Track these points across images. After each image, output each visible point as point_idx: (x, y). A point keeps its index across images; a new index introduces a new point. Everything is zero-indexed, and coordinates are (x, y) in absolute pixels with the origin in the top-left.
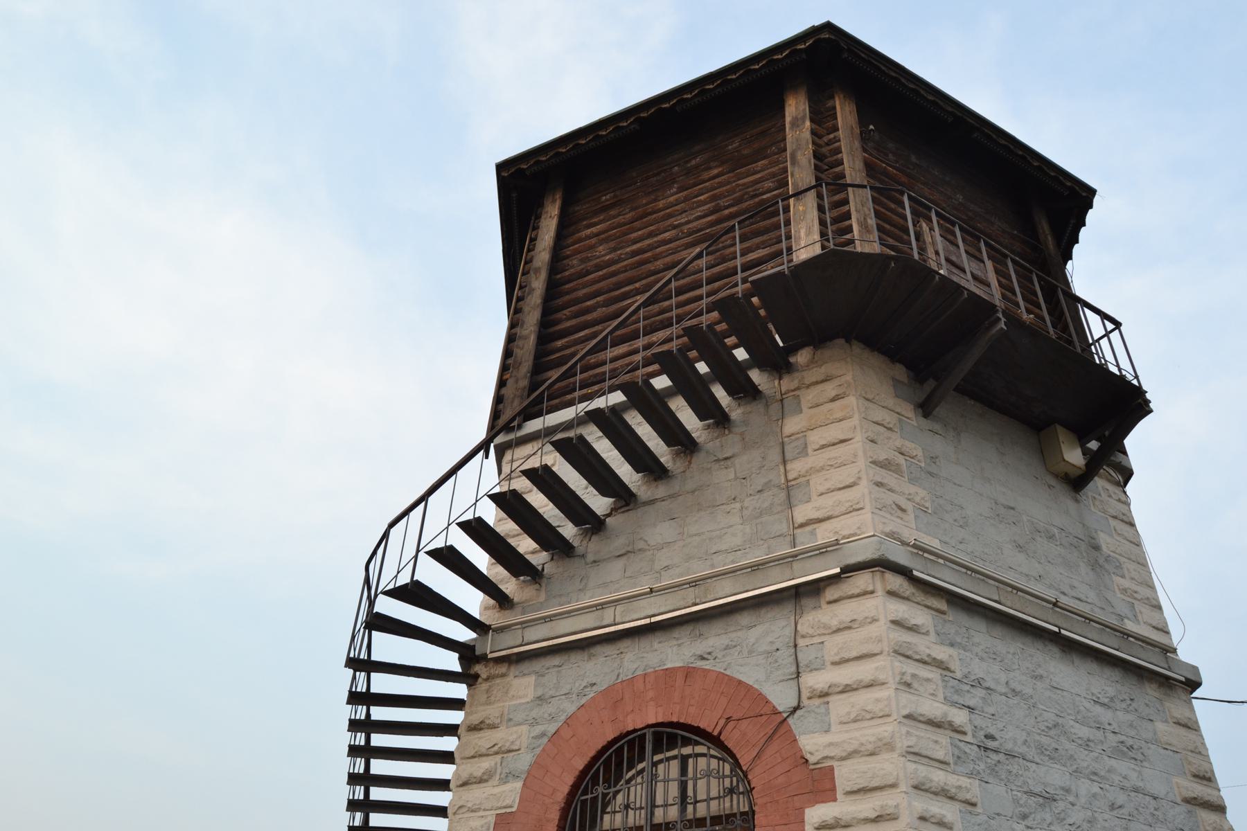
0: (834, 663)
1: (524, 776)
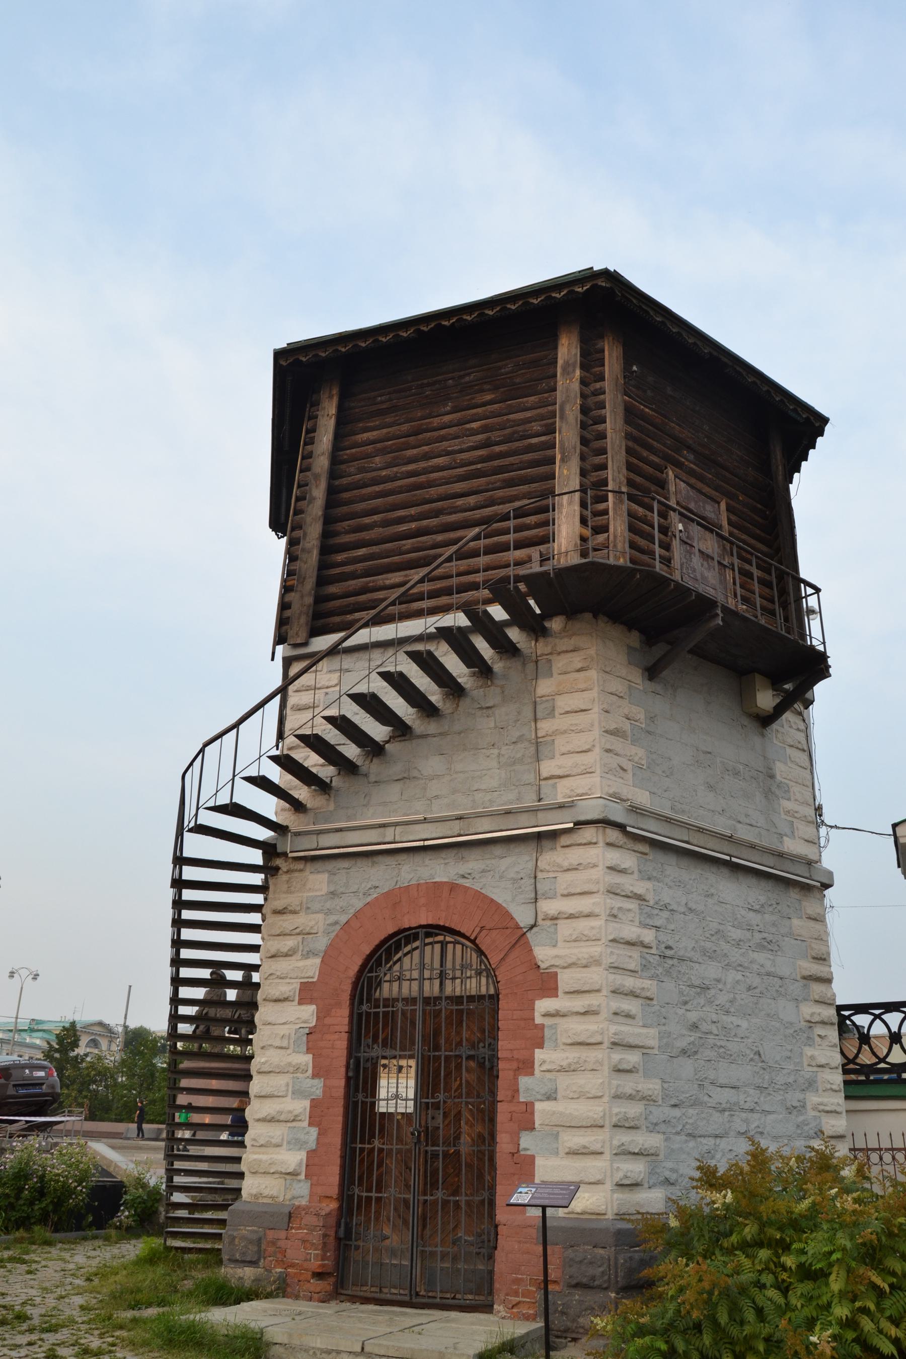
0: (563, 895)
1: (322, 954)
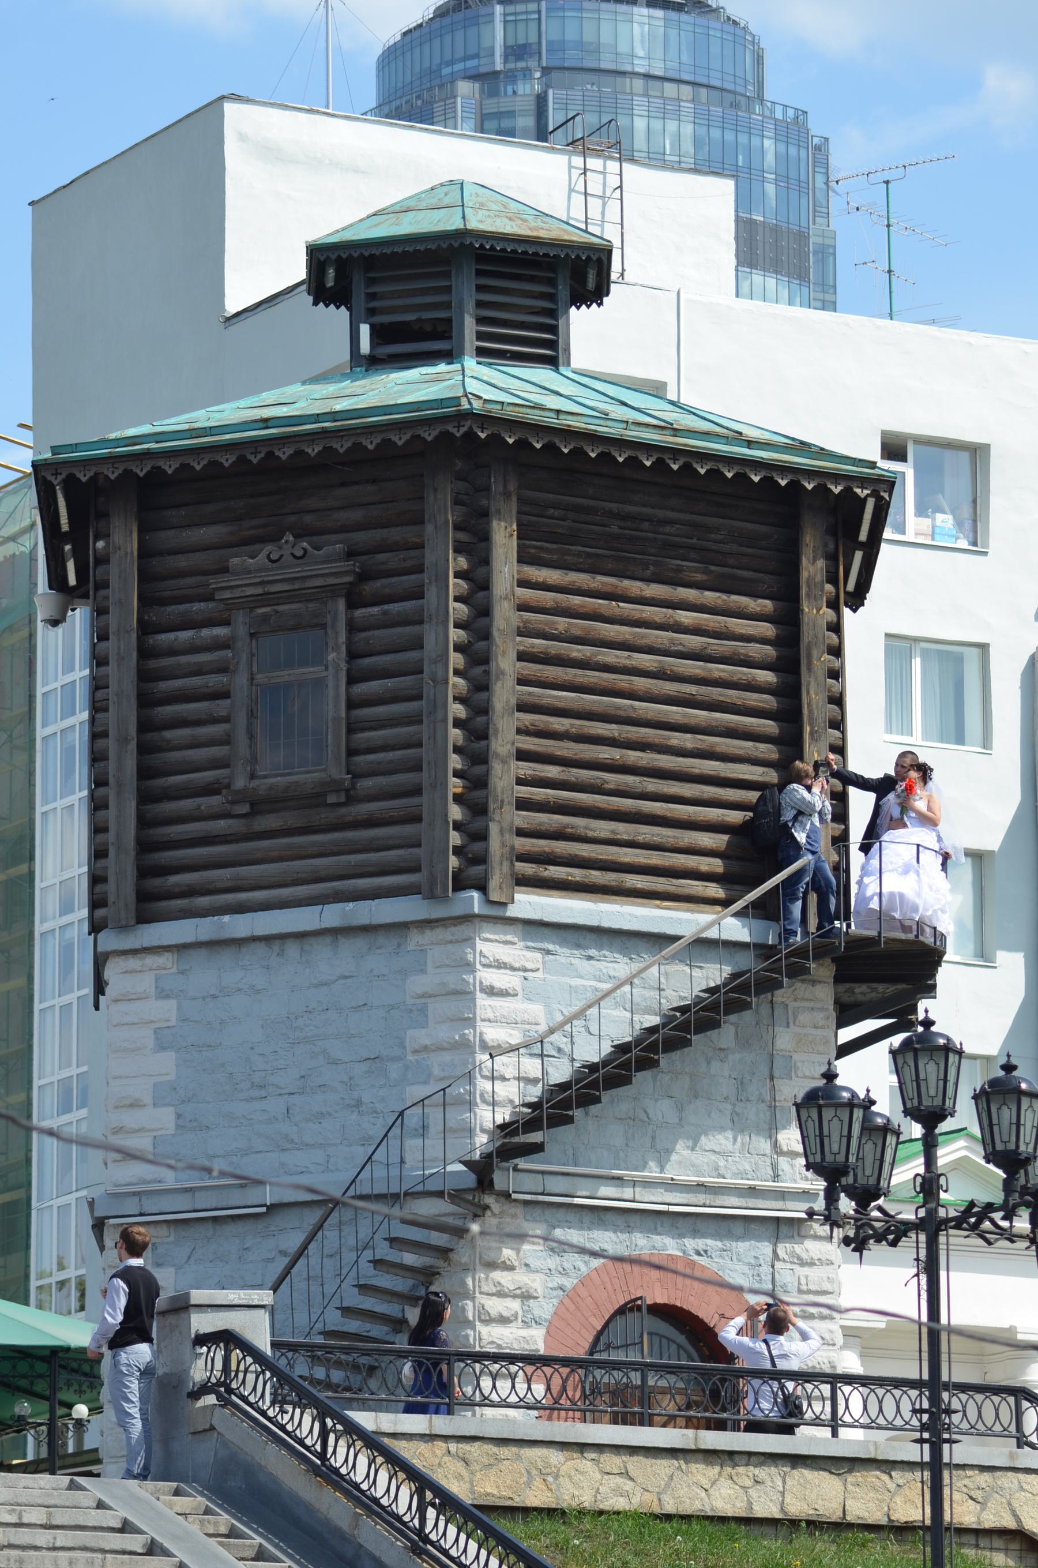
1: (546, 1324)
